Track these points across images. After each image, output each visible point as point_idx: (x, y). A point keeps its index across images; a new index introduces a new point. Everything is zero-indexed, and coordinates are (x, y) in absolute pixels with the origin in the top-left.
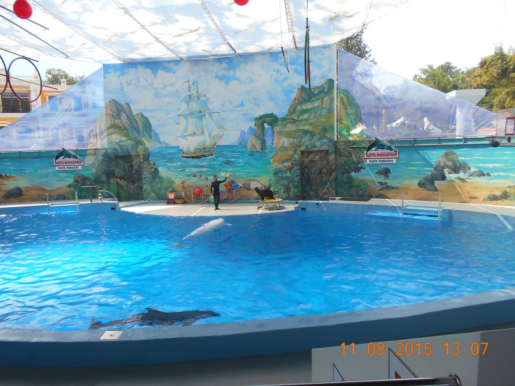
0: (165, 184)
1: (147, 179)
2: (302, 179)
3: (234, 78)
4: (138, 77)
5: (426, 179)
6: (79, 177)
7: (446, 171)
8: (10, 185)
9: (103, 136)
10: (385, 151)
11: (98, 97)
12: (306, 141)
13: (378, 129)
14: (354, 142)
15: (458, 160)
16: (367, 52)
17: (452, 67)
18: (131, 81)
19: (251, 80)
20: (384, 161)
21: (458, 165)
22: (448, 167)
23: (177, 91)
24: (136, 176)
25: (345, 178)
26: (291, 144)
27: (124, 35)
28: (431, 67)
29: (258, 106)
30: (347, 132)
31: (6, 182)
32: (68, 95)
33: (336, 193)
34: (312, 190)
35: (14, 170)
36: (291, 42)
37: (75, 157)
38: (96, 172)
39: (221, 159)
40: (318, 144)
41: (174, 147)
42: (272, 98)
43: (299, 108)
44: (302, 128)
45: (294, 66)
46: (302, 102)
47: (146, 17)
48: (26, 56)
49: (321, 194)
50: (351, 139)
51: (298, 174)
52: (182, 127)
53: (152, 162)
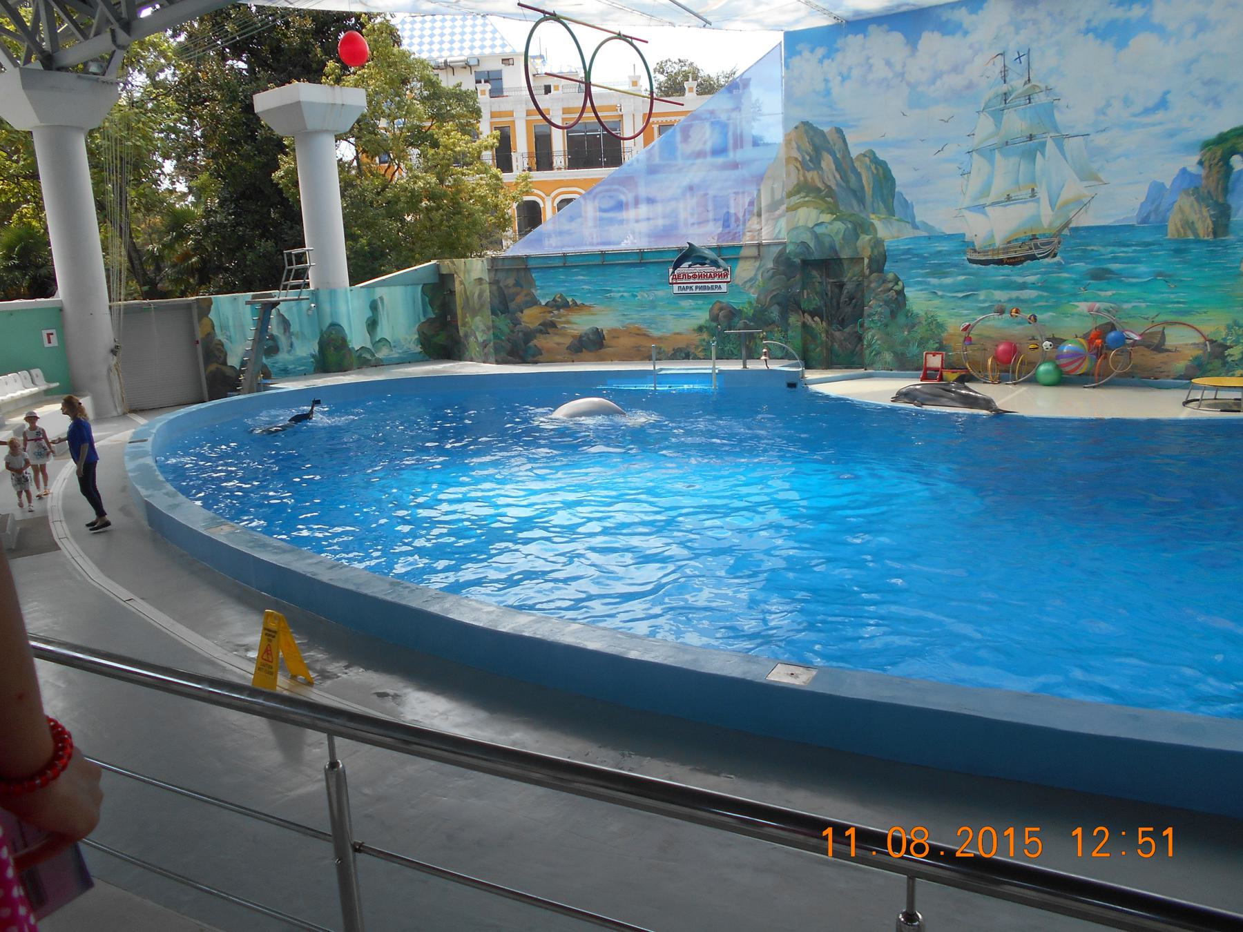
0: (920, 331)
1: (876, 318)
4: (868, 58)
6: (721, 309)
8: (581, 324)
23: (970, 86)
24: (848, 310)
35: (590, 292)
37: (714, 263)
38: (758, 300)
39: (1081, 266)
53: (890, 276)
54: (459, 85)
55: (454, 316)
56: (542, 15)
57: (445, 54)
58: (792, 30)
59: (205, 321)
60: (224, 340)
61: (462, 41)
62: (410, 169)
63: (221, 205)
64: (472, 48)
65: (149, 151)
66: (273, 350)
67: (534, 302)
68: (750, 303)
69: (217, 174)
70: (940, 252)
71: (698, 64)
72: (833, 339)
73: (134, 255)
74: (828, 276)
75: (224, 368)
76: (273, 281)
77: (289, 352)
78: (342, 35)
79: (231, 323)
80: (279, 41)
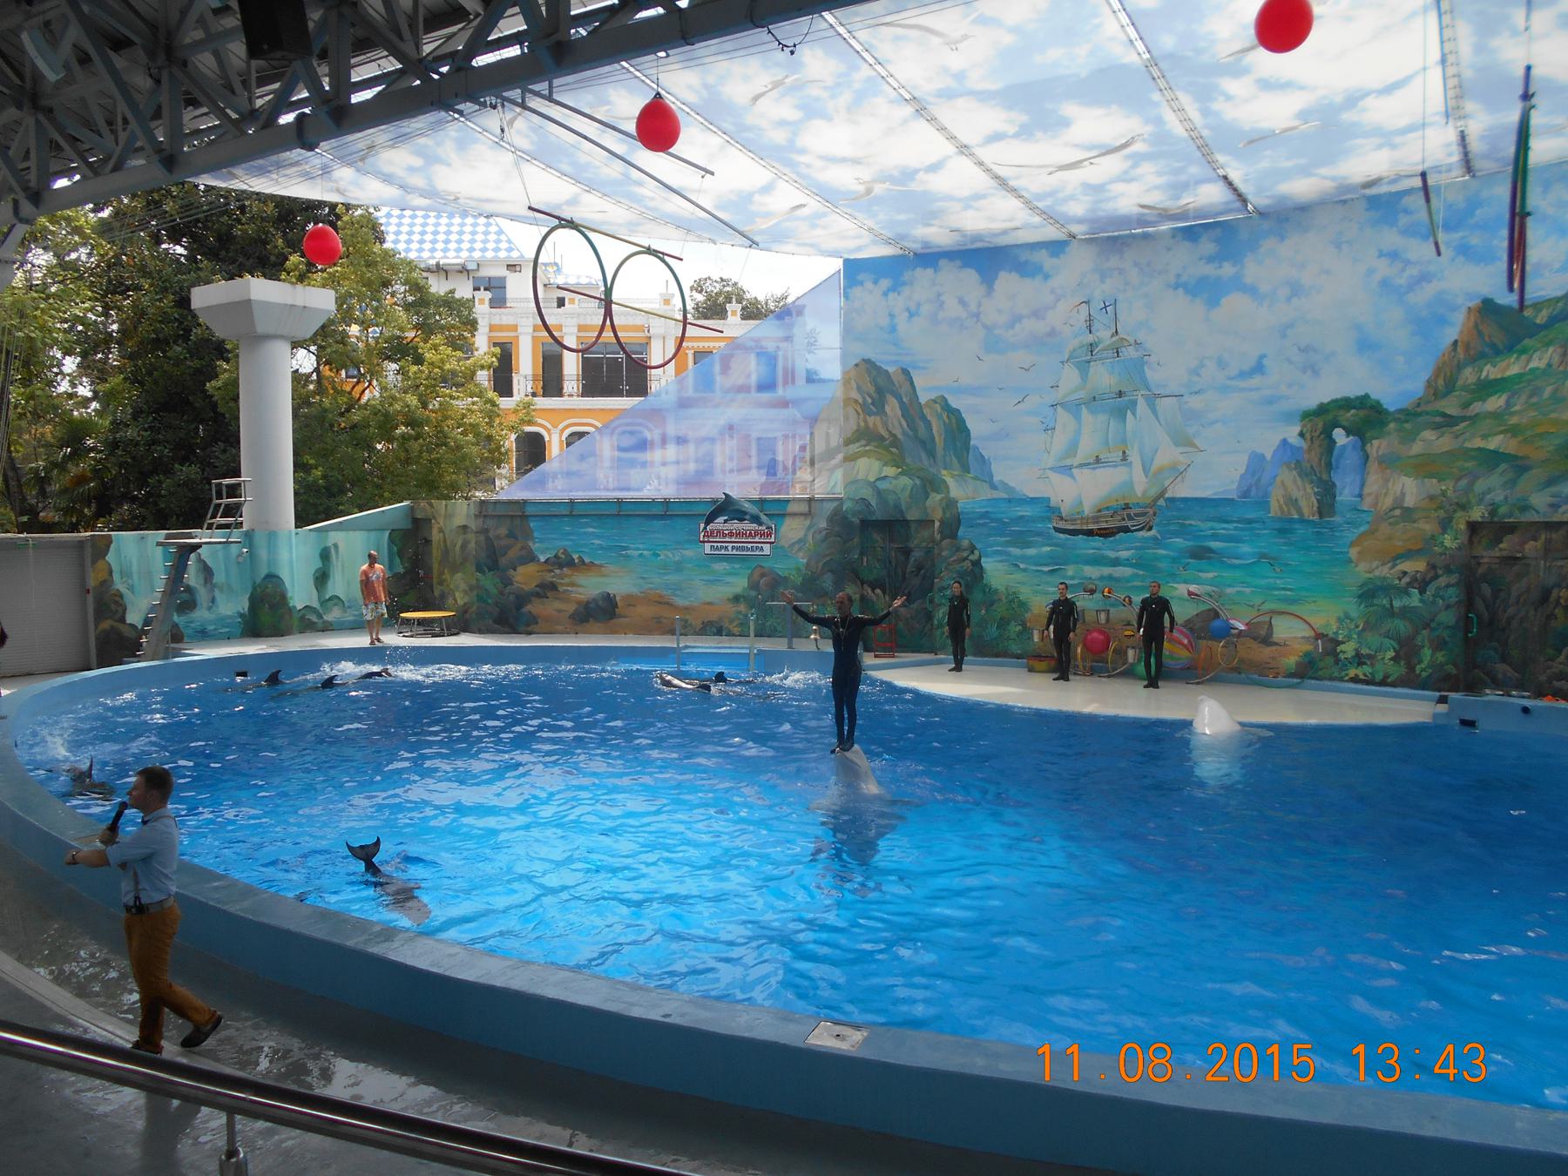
2: (1468, 620)
3: (1238, 285)
4: (939, 295)
6: (763, 575)
8: (589, 587)
9: (833, 462)
11: (825, 352)
12: (1490, 490)
18: (919, 305)
19: (1296, 290)
23: (1052, 333)
24: (916, 581)
26: (1432, 498)
27: (908, 175)
29: (1316, 372)
32: (746, 349)
34: (1504, 660)
35: (601, 548)
36: (1450, 155)
37: (756, 519)
38: (808, 564)
40: (1540, 500)
41: (1034, 500)
42: (1365, 345)
44: (1478, 443)
45: (1456, 236)
46: (1482, 355)
47: (973, 121)
49: (1543, 678)
51: (1454, 600)
52: (1060, 441)
53: (965, 543)
54: (452, 292)
55: (431, 569)
56: (556, 222)
57: (438, 255)
58: (852, 257)
59: (100, 564)
60: (123, 589)
61: (460, 242)
62: (384, 388)
63: (135, 416)
64: (471, 250)
65: (45, 344)
66: (189, 605)
67: (531, 558)
69: (135, 380)
70: (1022, 517)
71: (744, 284)
73: (10, 474)
75: (121, 626)
76: (195, 516)
77: (209, 608)
78: (311, 226)
79: (135, 568)
80: (232, 227)
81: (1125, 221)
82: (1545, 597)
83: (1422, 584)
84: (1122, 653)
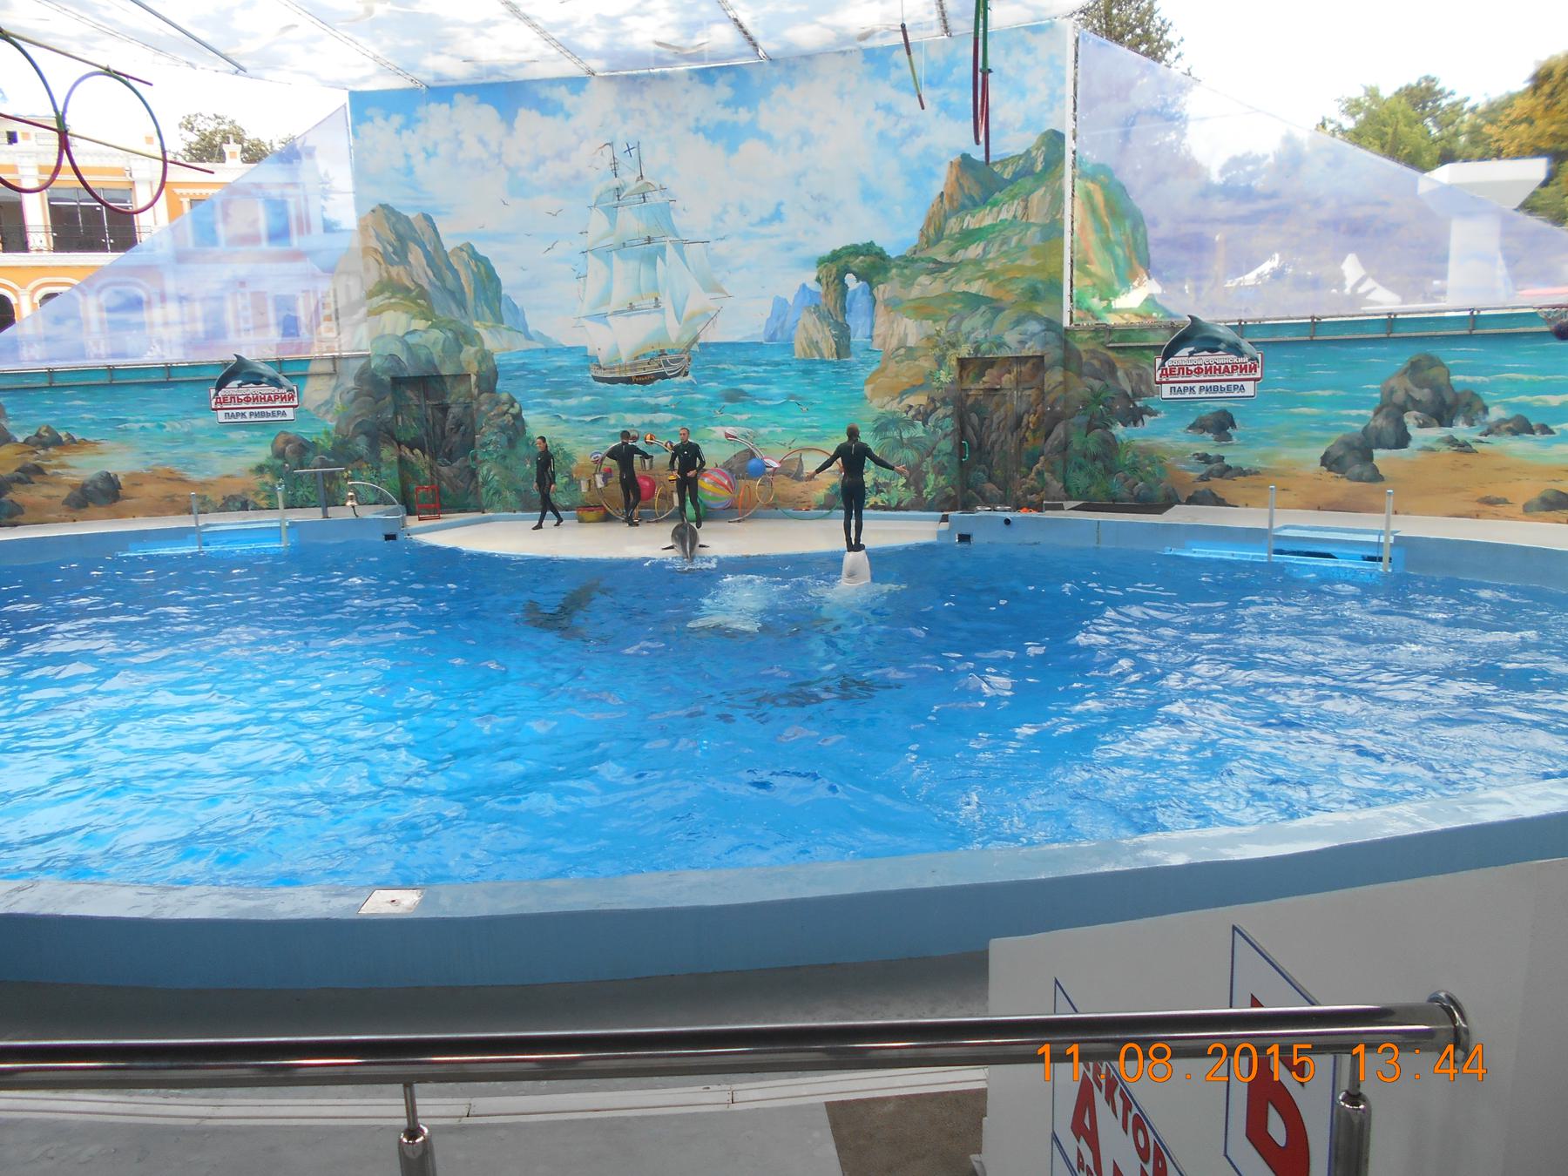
1: (491, 448)
4: (457, 133)
5: (1348, 445)
6: (288, 442)
7: (1410, 419)
8: (83, 468)
9: (356, 317)
10: (1222, 358)
12: (974, 330)
13: (1197, 290)
14: (1126, 332)
15: (1450, 387)
16: (1169, 46)
17: (1440, 92)
19: (806, 139)
20: (1215, 389)
21: (1449, 399)
22: (1417, 404)
23: (577, 176)
24: (456, 439)
25: (1092, 442)
26: (929, 338)
28: (1373, 94)
29: (827, 220)
30: (1101, 299)
31: (71, 459)
33: (1067, 489)
34: (990, 479)
35: (94, 422)
36: (930, 13)
37: (274, 382)
38: (338, 430)
39: (713, 386)
40: (1011, 338)
41: (570, 350)
42: (869, 195)
43: (953, 225)
45: (939, 92)
46: (964, 207)
48: (113, 68)
49: (1019, 493)
50: (1112, 320)
51: (950, 429)
53: (504, 396)
58: (359, 88)
68: (327, 433)
72: (440, 477)
74: (427, 397)
81: (640, 58)
82: (1019, 419)
83: (924, 416)
84: (666, 497)
